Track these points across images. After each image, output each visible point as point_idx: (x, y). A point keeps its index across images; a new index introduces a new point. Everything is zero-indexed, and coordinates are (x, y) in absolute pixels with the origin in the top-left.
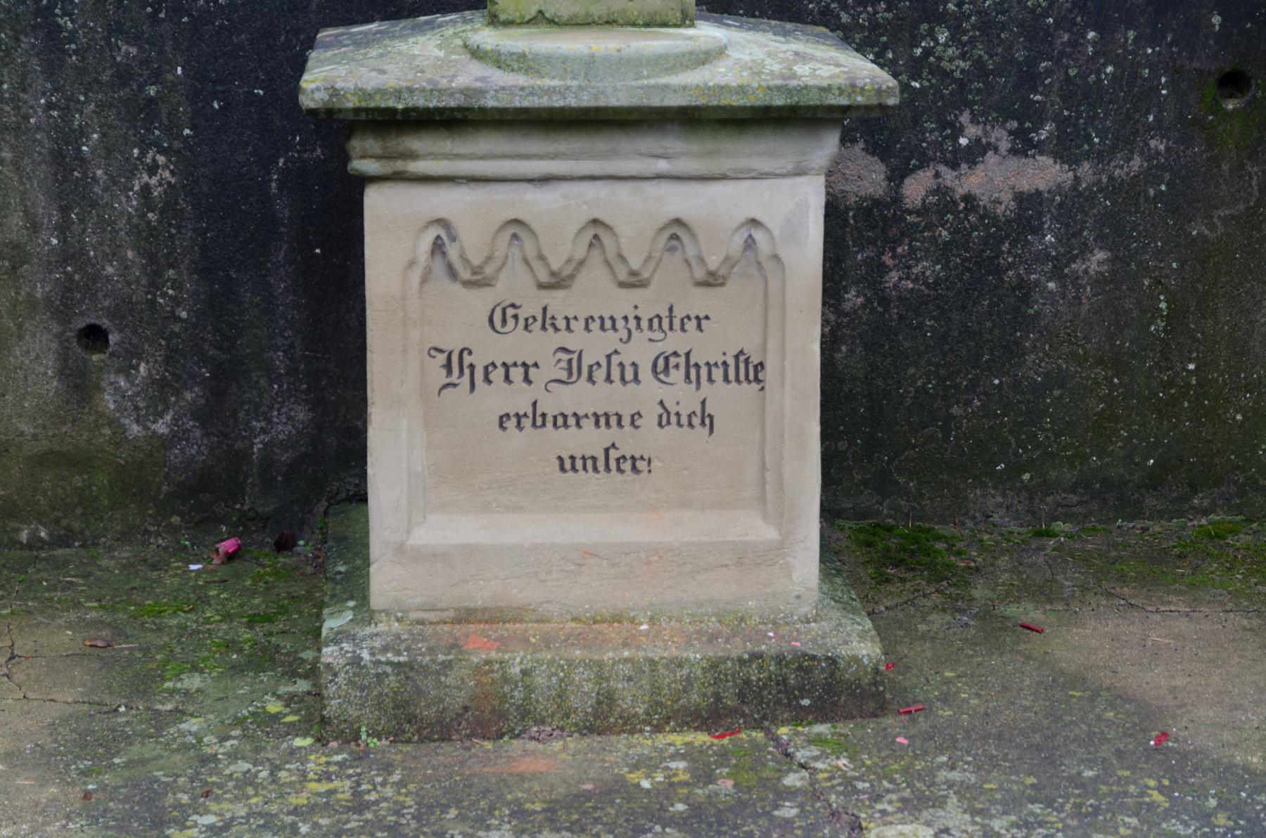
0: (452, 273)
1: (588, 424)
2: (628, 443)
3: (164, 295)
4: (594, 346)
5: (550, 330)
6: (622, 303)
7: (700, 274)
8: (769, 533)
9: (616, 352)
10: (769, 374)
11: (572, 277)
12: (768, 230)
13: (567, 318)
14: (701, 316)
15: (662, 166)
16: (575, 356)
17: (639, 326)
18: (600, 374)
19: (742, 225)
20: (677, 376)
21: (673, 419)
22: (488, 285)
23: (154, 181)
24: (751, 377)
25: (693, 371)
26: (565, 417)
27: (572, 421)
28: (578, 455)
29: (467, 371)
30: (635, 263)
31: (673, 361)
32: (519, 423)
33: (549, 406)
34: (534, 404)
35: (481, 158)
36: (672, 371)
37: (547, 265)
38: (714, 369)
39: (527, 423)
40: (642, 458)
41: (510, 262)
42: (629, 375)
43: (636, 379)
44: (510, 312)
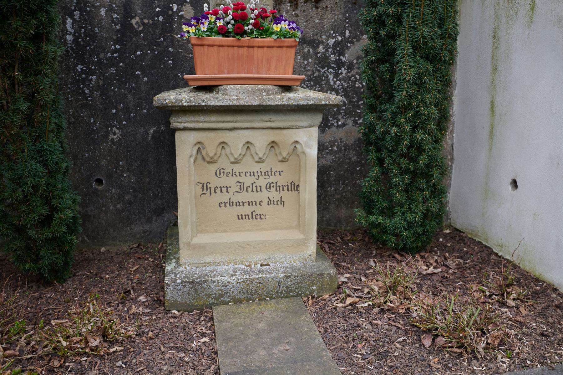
0: (204, 159)
1: (246, 205)
2: (259, 210)
3: (119, 170)
4: (248, 181)
5: (234, 176)
6: (256, 168)
7: (280, 158)
8: (301, 236)
9: (255, 182)
10: (301, 188)
11: (241, 160)
12: (301, 144)
13: (239, 172)
14: (281, 171)
16: (242, 184)
17: (261, 174)
18: (250, 189)
19: (293, 143)
20: (273, 189)
21: (272, 202)
22: (215, 163)
23: (115, 137)
24: (296, 189)
25: (278, 188)
26: (239, 203)
27: (241, 204)
28: (243, 214)
29: (209, 190)
30: (261, 156)
31: (272, 185)
32: (225, 205)
33: (234, 200)
34: (230, 199)
35: (213, 122)
36: (272, 188)
37: (233, 156)
38: (284, 187)
39: (227, 205)
40: (263, 215)
41: (222, 155)
42: (259, 190)
43: (261, 190)
44: (222, 171)
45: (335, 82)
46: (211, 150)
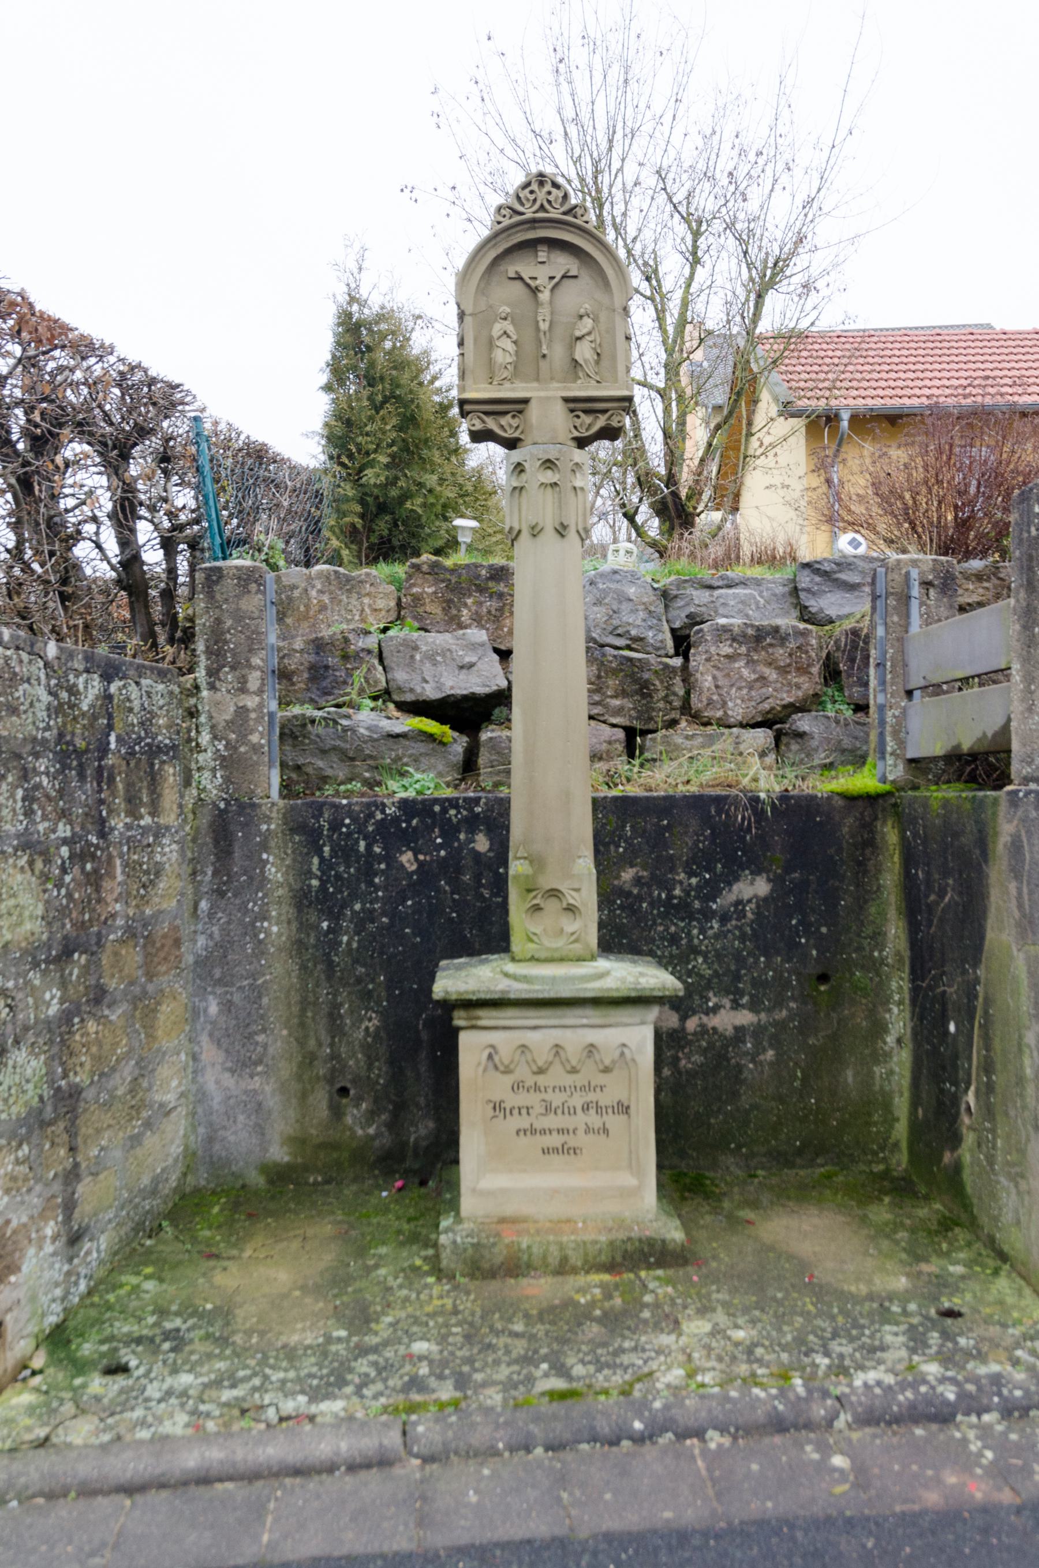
0: (496, 1068)
1: (555, 1133)
2: (572, 1141)
4: (557, 1099)
6: (569, 1080)
7: (601, 1067)
8: (633, 1182)
10: (632, 1110)
15: (585, 1021)
20: (592, 1111)
30: (574, 1063)
33: (538, 1125)
45: (701, 941)
46: (505, 1054)
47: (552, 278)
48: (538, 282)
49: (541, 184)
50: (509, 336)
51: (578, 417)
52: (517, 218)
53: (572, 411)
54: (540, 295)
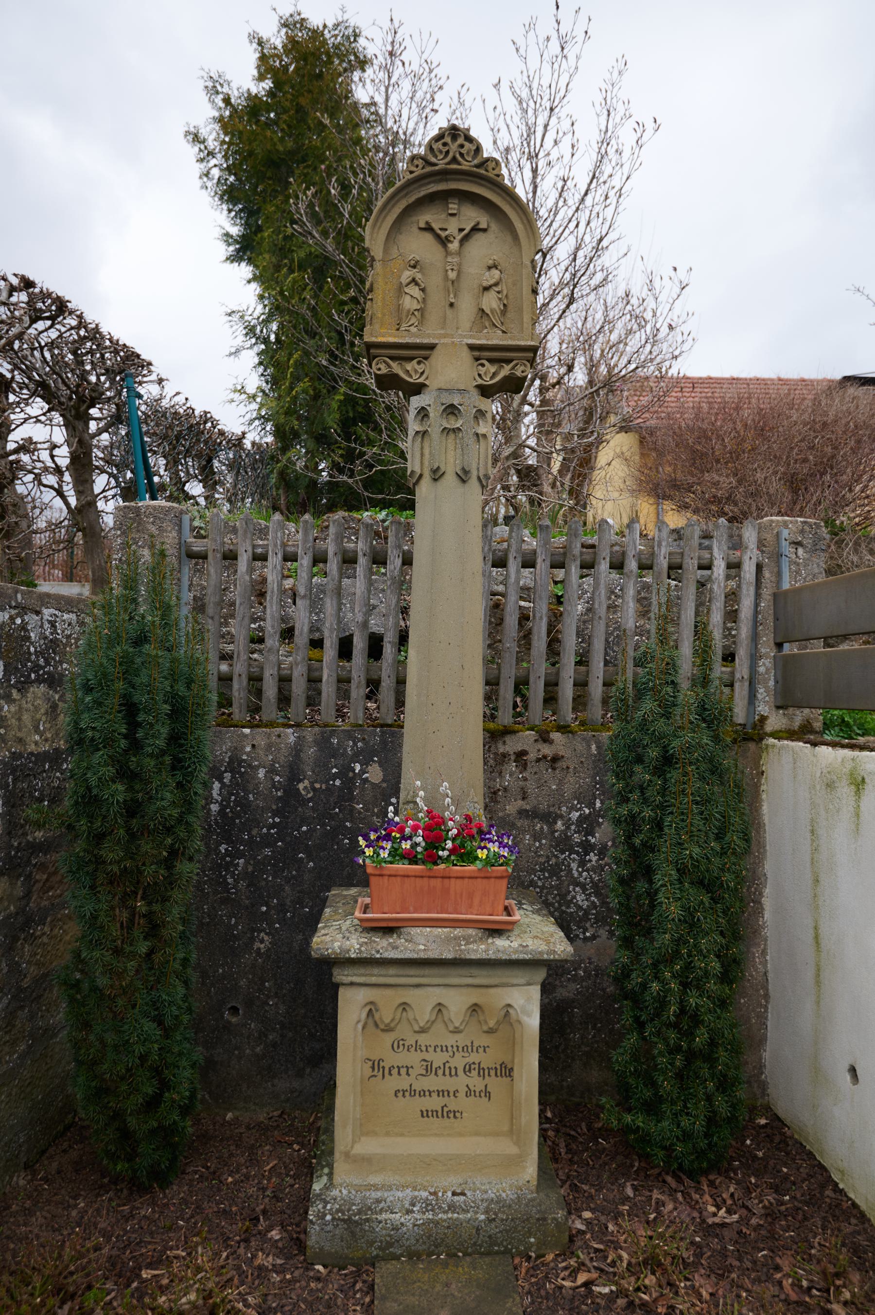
0: (376, 1025)
1: (434, 1095)
4: (438, 1059)
6: (450, 1040)
7: (485, 1028)
8: (513, 1150)
10: (515, 1073)
11: (429, 1028)
15: (470, 981)
18: (440, 1072)
20: (474, 1073)
23: (262, 946)
27: (427, 1093)
30: (457, 1025)
33: (417, 1087)
39: (407, 1094)
42: (453, 1073)
43: (456, 1074)
45: (580, 874)
46: (386, 1015)
47: (461, 230)
48: (447, 233)
49: (454, 137)
50: (417, 284)
51: (483, 365)
52: (429, 169)
53: (477, 359)
54: (450, 245)
